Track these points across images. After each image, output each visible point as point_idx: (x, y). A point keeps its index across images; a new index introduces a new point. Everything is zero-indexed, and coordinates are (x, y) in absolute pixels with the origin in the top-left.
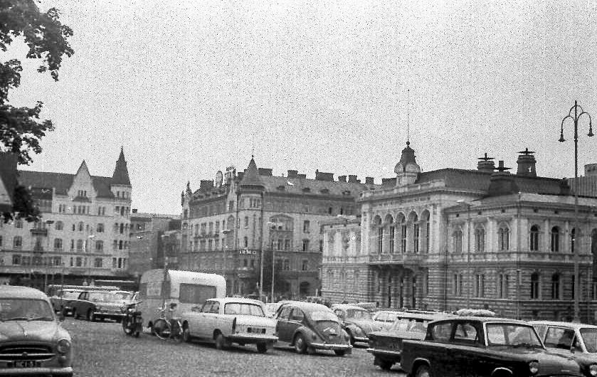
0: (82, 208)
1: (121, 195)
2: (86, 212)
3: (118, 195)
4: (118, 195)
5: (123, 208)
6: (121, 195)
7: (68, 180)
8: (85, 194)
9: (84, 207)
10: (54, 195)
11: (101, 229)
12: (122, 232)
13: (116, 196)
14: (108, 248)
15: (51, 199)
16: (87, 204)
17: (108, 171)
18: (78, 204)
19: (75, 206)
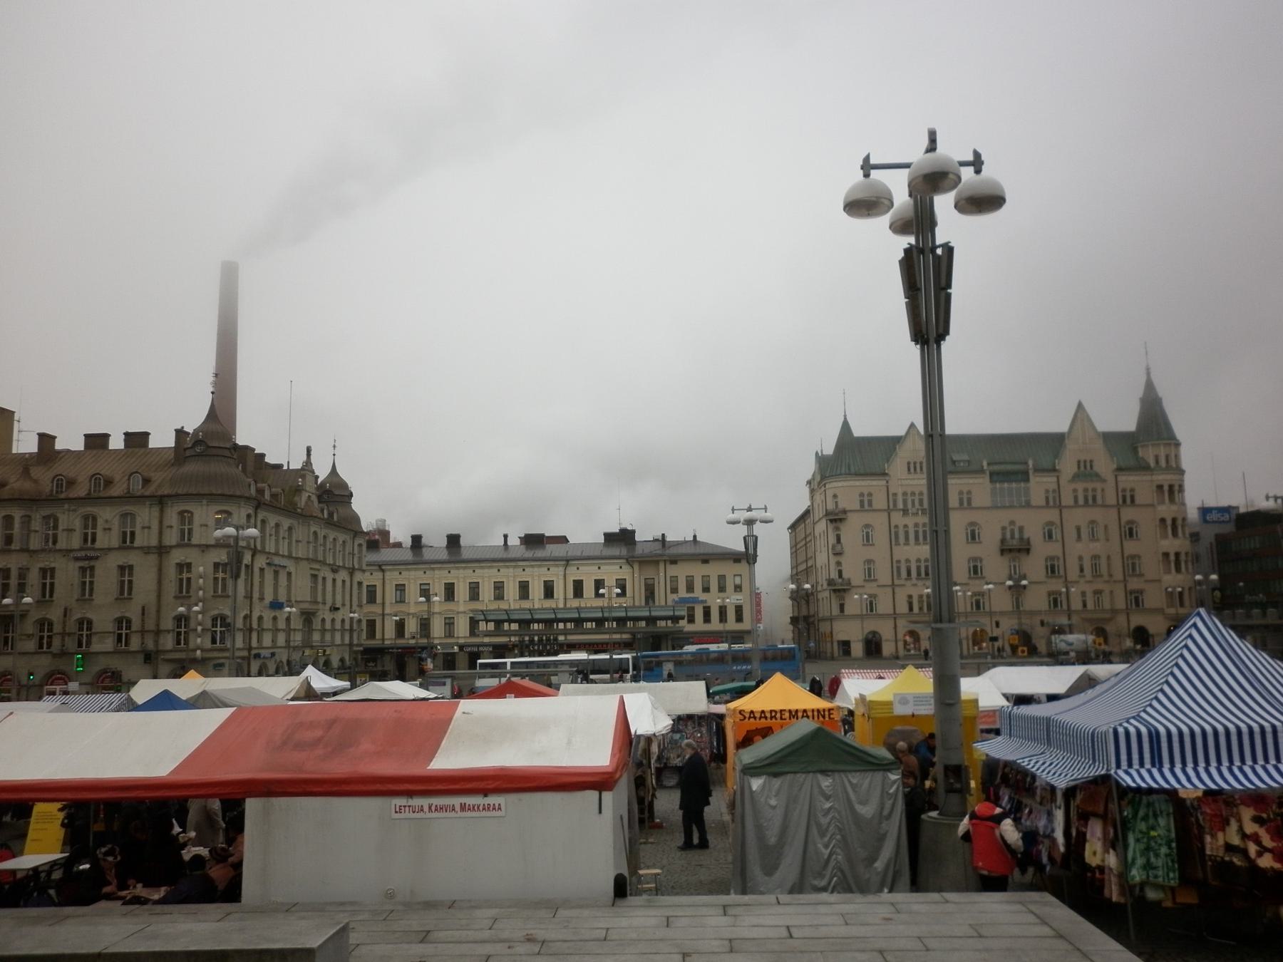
0: (1090, 494)
1: (1163, 463)
2: (1099, 501)
3: (1157, 462)
4: (1157, 462)
5: (1171, 487)
6: (1163, 463)
7: (1055, 442)
8: (1091, 467)
9: (1094, 490)
10: (1031, 472)
11: (1130, 532)
12: (1175, 534)
13: (1152, 464)
14: (1151, 566)
15: (1027, 480)
16: (1098, 486)
17: (1126, 421)
18: (1080, 486)
19: (1075, 491)
